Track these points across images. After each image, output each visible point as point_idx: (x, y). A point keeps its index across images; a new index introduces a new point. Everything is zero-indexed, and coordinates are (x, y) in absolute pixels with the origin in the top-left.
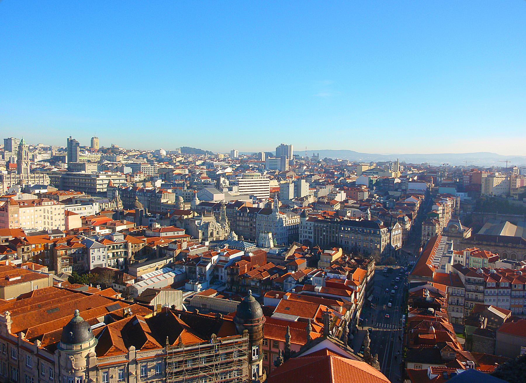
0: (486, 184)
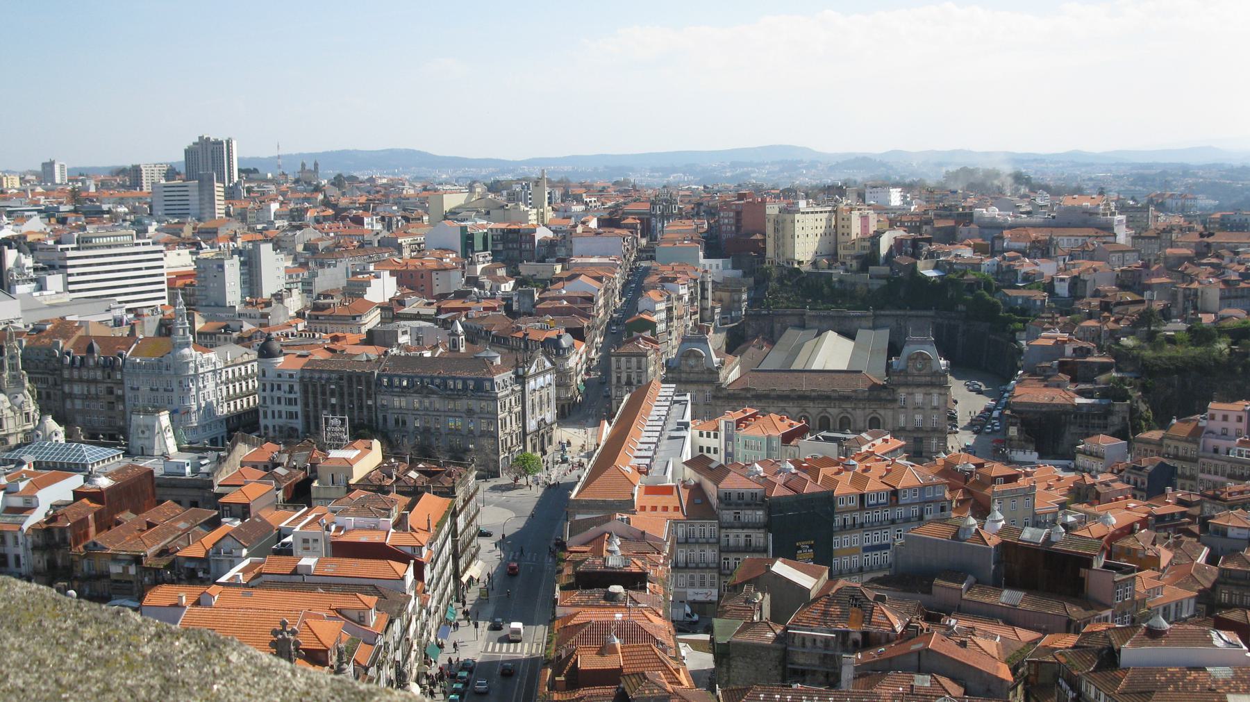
0: (776, 230)
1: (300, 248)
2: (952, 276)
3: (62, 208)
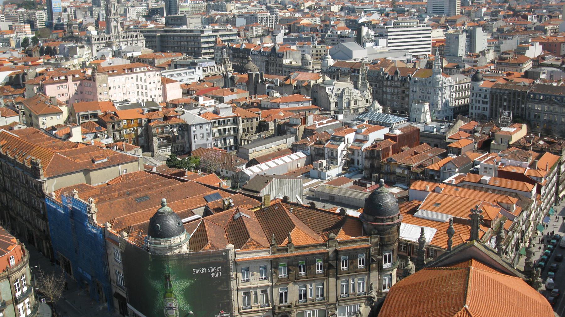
1: (495, 30)
3: (387, 9)
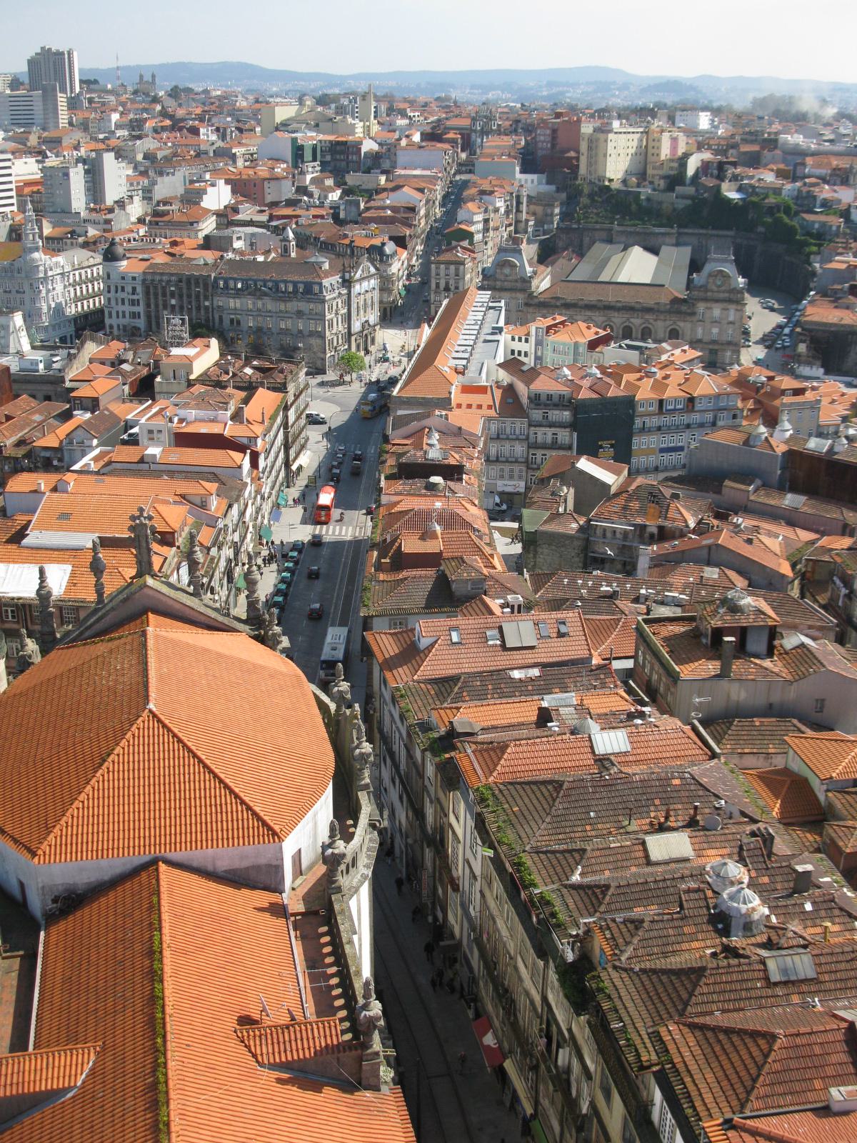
0: (590, 148)
1: (140, 157)
2: (754, 199)
